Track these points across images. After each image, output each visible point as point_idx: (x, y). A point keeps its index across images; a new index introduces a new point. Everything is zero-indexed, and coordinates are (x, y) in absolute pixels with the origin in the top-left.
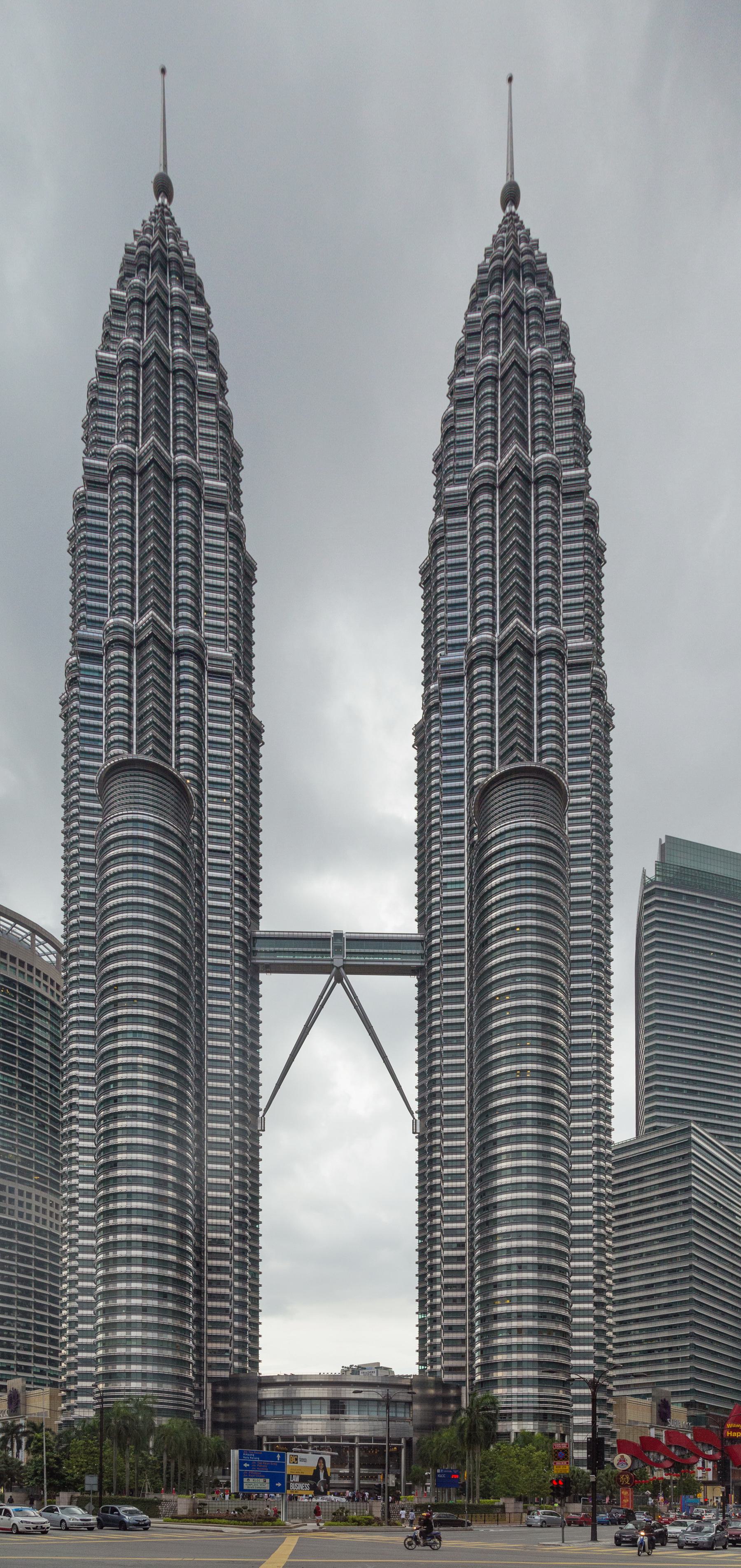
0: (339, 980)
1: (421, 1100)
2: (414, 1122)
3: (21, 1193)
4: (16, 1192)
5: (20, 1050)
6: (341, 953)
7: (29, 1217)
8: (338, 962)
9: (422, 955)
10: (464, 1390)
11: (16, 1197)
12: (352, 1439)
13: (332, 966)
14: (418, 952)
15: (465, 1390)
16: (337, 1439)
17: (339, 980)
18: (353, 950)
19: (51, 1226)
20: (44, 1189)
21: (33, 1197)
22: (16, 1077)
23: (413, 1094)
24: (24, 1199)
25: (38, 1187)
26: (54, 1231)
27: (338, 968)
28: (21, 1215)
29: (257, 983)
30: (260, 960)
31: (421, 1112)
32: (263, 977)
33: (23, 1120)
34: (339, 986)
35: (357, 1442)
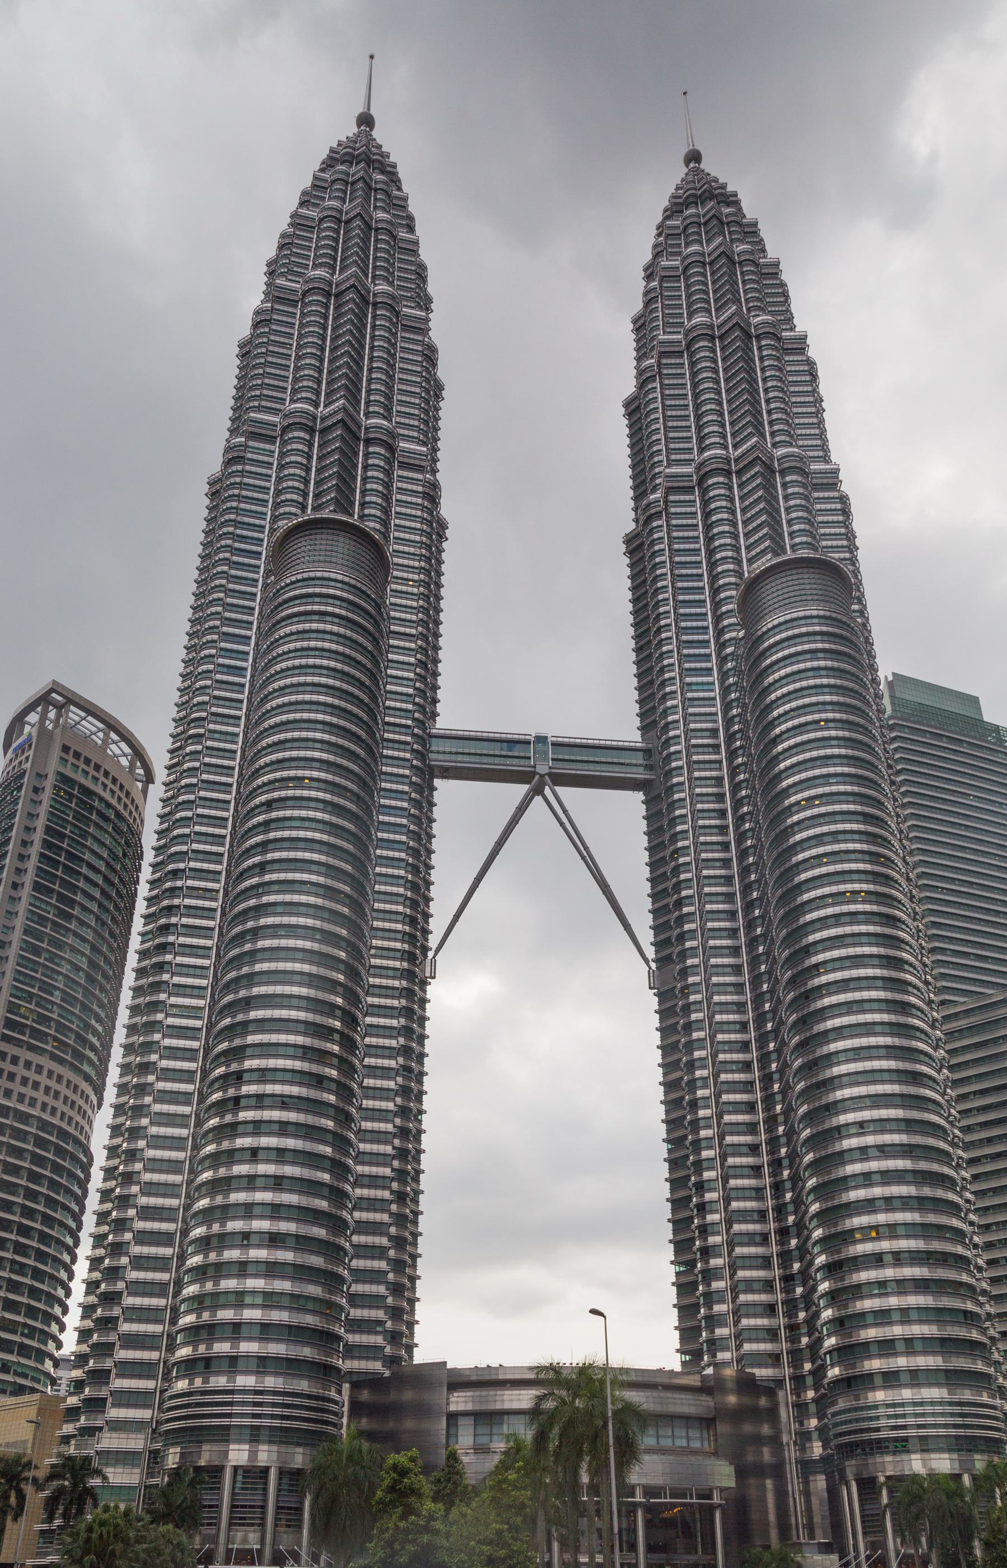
3: (28, 1064)
4: (21, 1063)
5: (65, 865)
6: (546, 759)
7: (33, 1102)
8: (542, 769)
10: (781, 1394)
11: (20, 1071)
13: (534, 773)
15: (785, 1396)
17: (538, 791)
18: (560, 757)
19: (62, 1119)
20: (61, 1061)
21: (45, 1072)
22: (53, 902)
24: (32, 1075)
25: (54, 1057)
26: (64, 1125)
27: (542, 776)
28: (21, 1098)
29: (432, 789)
30: (436, 759)
32: (437, 782)
33: (51, 960)
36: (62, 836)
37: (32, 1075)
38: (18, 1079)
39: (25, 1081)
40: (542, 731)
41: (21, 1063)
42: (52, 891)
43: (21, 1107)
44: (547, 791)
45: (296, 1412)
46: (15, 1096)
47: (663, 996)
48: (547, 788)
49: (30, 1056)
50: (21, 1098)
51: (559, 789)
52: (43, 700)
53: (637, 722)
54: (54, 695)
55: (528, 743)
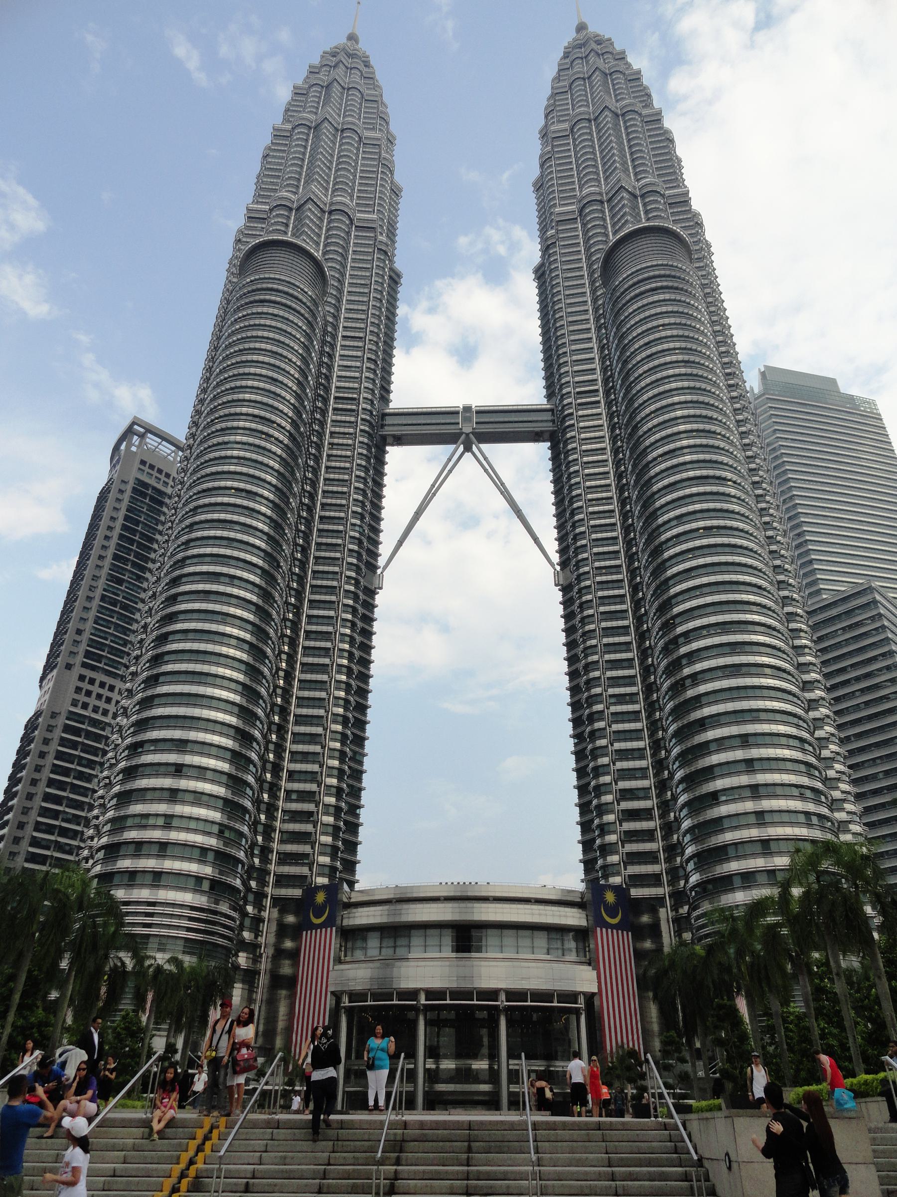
1: (562, 551)
2: (556, 574)
12: (493, 994)
16: (466, 994)
17: (468, 449)
23: (552, 546)
24: (105, 692)
28: (96, 709)
31: (564, 564)
34: (468, 455)
35: (502, 1002)
36: (137, 523)
37: (105, 692)
38: (94, 695)
39: (99, 696)
41: (97, 683)
42: (128, 560)
43: (94, 716)
44: (474, 448)
45: (166, 921)
46: (90, 708)
47: (566, 589)
48: (474, 447)
49: (109, 681)
50: (96, 709)
51: (483, 446)
52: (129, 433)
53: (544, 392)
54: (136, 427)
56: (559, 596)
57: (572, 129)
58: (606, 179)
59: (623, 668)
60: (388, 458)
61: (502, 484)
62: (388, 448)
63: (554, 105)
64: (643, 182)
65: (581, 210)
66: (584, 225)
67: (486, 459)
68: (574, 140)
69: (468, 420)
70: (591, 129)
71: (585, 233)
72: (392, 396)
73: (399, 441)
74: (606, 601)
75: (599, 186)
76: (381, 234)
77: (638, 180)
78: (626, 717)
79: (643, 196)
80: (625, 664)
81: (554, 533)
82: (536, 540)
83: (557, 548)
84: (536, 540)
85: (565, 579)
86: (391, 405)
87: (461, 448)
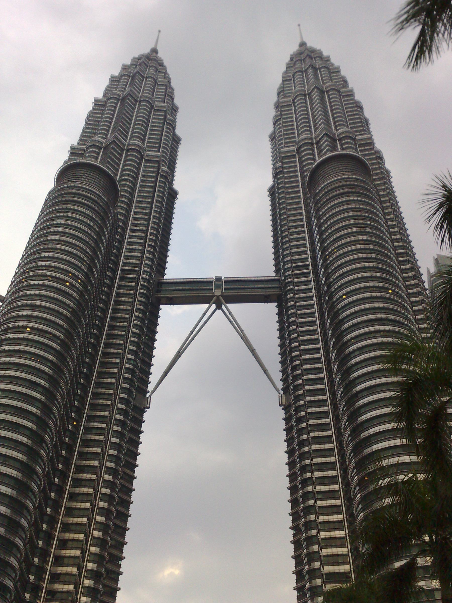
0: (219, 307)
1: (284, 380)
9: (279, 287)
14: (277, 285)
17: (219, 307)
23: (277, 376)
27: (218, 297)
29: (159, 309)
31: (285, 389)
34: (219, 312)
40: (219, 275)
48: (223, 306)
55: (212, 282)
56: (282, 414)
57: (294, 100)
58: (315, 131)
59: (328, 470)
60: (160, 313)
61: (242, 331)
62: (161, 306)
63: (283, 87)
64: (340, 131)
65: (298, 149)
66: (300, 158)
67: (230, 313)
68: (295, 107)
69: (218, 287)
70: (306, 100)
71: (301, 163)
72: (166, 271)
73: (171, 301)
74: (314, 416)
75: (311, 134)
76: (164, 166)
77: (337, 130)
78: (330, 510)
79: (340, 140)
80: (329, 466)
81: (279, 367)
82: (265, 371)
83: (281, 377)
84: (265, 371)
85: (287, 400)
86: (165, 277)
87: (214, 306)
